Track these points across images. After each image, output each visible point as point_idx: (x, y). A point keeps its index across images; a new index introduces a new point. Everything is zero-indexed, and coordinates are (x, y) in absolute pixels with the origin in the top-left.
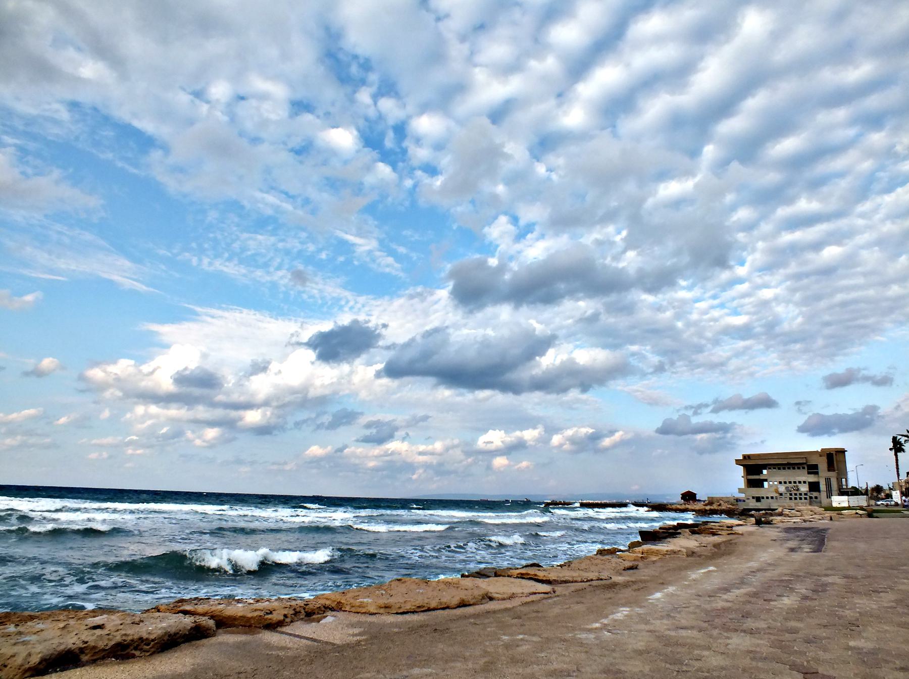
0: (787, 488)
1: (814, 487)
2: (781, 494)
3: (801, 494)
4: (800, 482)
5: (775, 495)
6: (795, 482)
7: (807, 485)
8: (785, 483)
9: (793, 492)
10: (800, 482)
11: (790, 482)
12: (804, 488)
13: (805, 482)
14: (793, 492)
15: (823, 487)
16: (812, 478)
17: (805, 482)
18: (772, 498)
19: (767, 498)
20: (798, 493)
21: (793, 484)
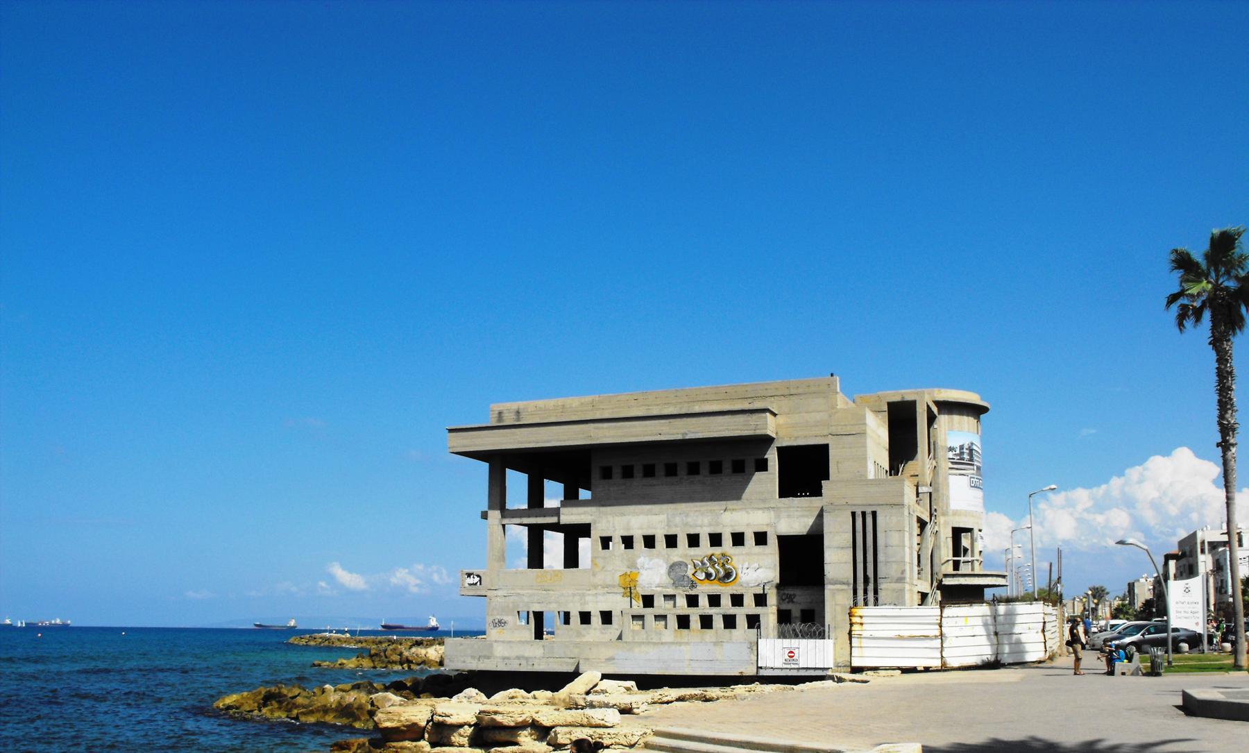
0: (672, 567)
1: (801, 559)
2: (648, 601)
3: (737, 600)
4: (738, 539)
5: (617, 603)
6: (716, 540)
7: (771, 552)
8: (671, 541)
9: (704, 590)
10: (738, 539)
11: (694, 540)
12: (759, 569)
13: (761, 538)
14: (704, 590)
15: (837, 560)
16: (794, 518)
17: (761, 538)
18: (607, 617)
19: (585, 618)
20: (725, 591)
21: (705, 546)
